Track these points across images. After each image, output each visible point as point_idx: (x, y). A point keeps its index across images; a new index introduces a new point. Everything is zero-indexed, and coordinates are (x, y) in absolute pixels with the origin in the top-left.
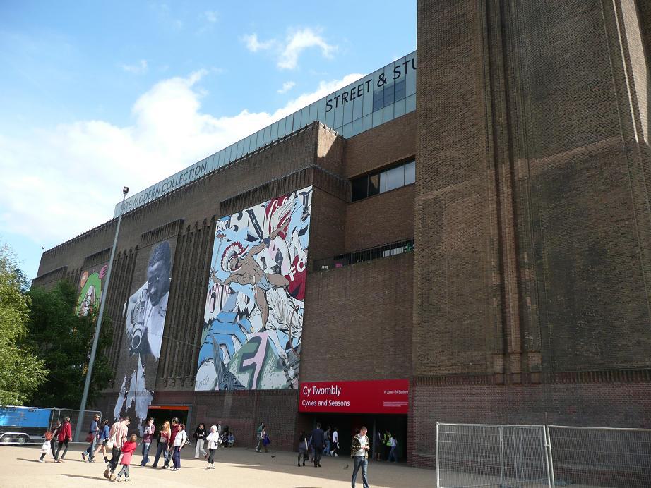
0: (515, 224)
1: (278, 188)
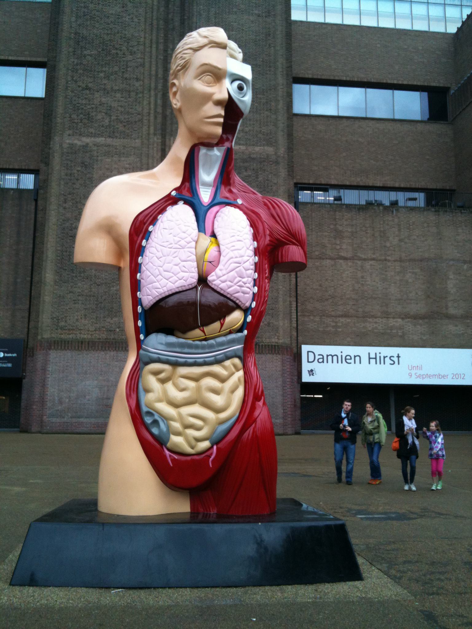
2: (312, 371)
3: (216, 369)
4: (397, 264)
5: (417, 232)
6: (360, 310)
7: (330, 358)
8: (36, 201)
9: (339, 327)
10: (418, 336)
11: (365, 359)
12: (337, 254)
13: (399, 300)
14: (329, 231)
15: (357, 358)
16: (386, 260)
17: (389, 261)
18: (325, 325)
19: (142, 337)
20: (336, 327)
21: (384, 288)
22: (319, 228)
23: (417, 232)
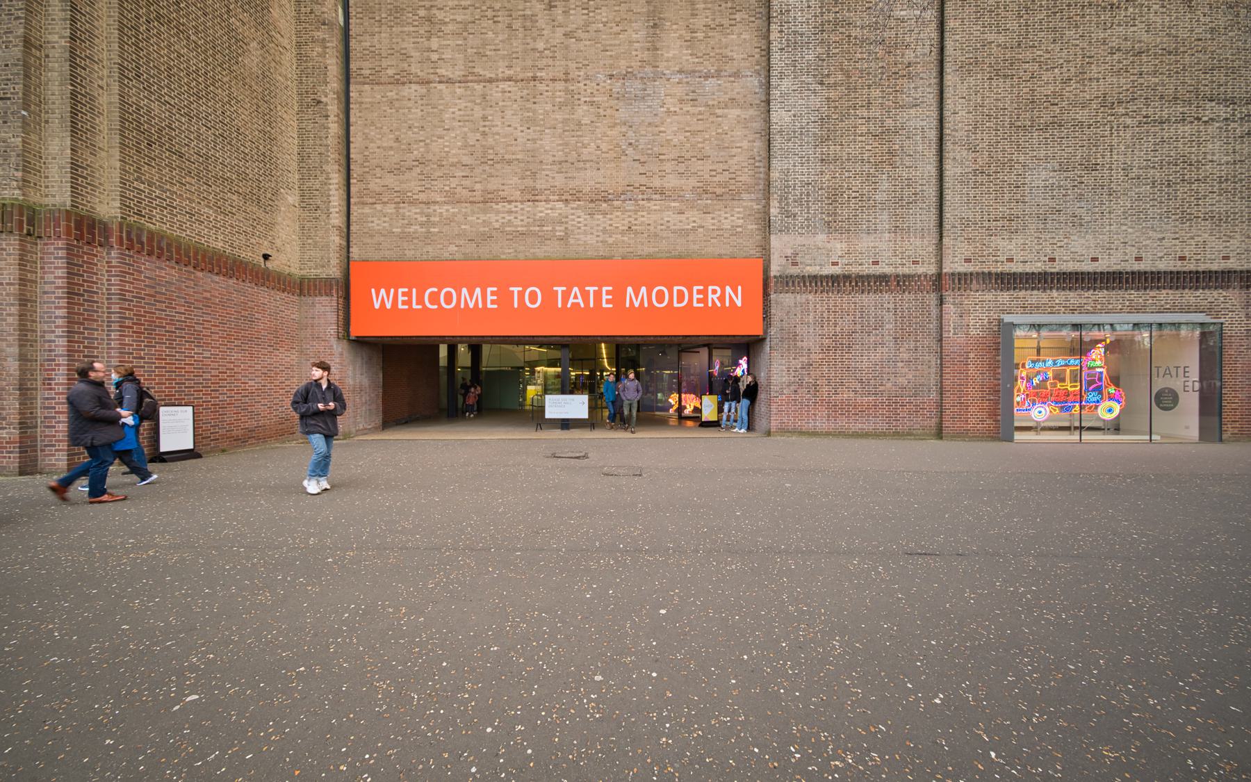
4: (560, 85)
5: (604, 14)
6: (478, 186)
9: (434, 224)
10: (598, 236)
12: (432, 71)
13: (560, 163)
14: (416, 23)
16: (534, 78)
17: (541, 80)
18: (406, 222)
20: (428, 224)
21: (528, 140)
22: (395, 18)
23: (604, 14)
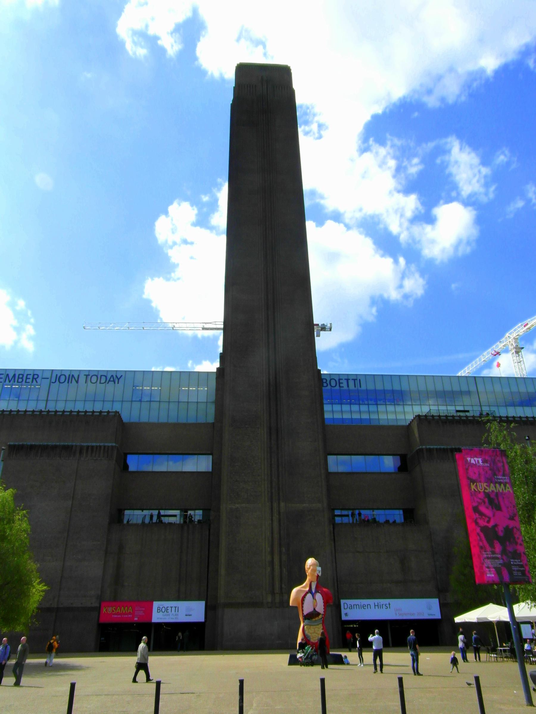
0: (280, 533)
1: (81, 452)
2: (346, 614)
3: (317, 626)
7: (355, 606)
8: (209, 530)
11: (372, 606)
15: (369, 606)
19: (304, 620)
